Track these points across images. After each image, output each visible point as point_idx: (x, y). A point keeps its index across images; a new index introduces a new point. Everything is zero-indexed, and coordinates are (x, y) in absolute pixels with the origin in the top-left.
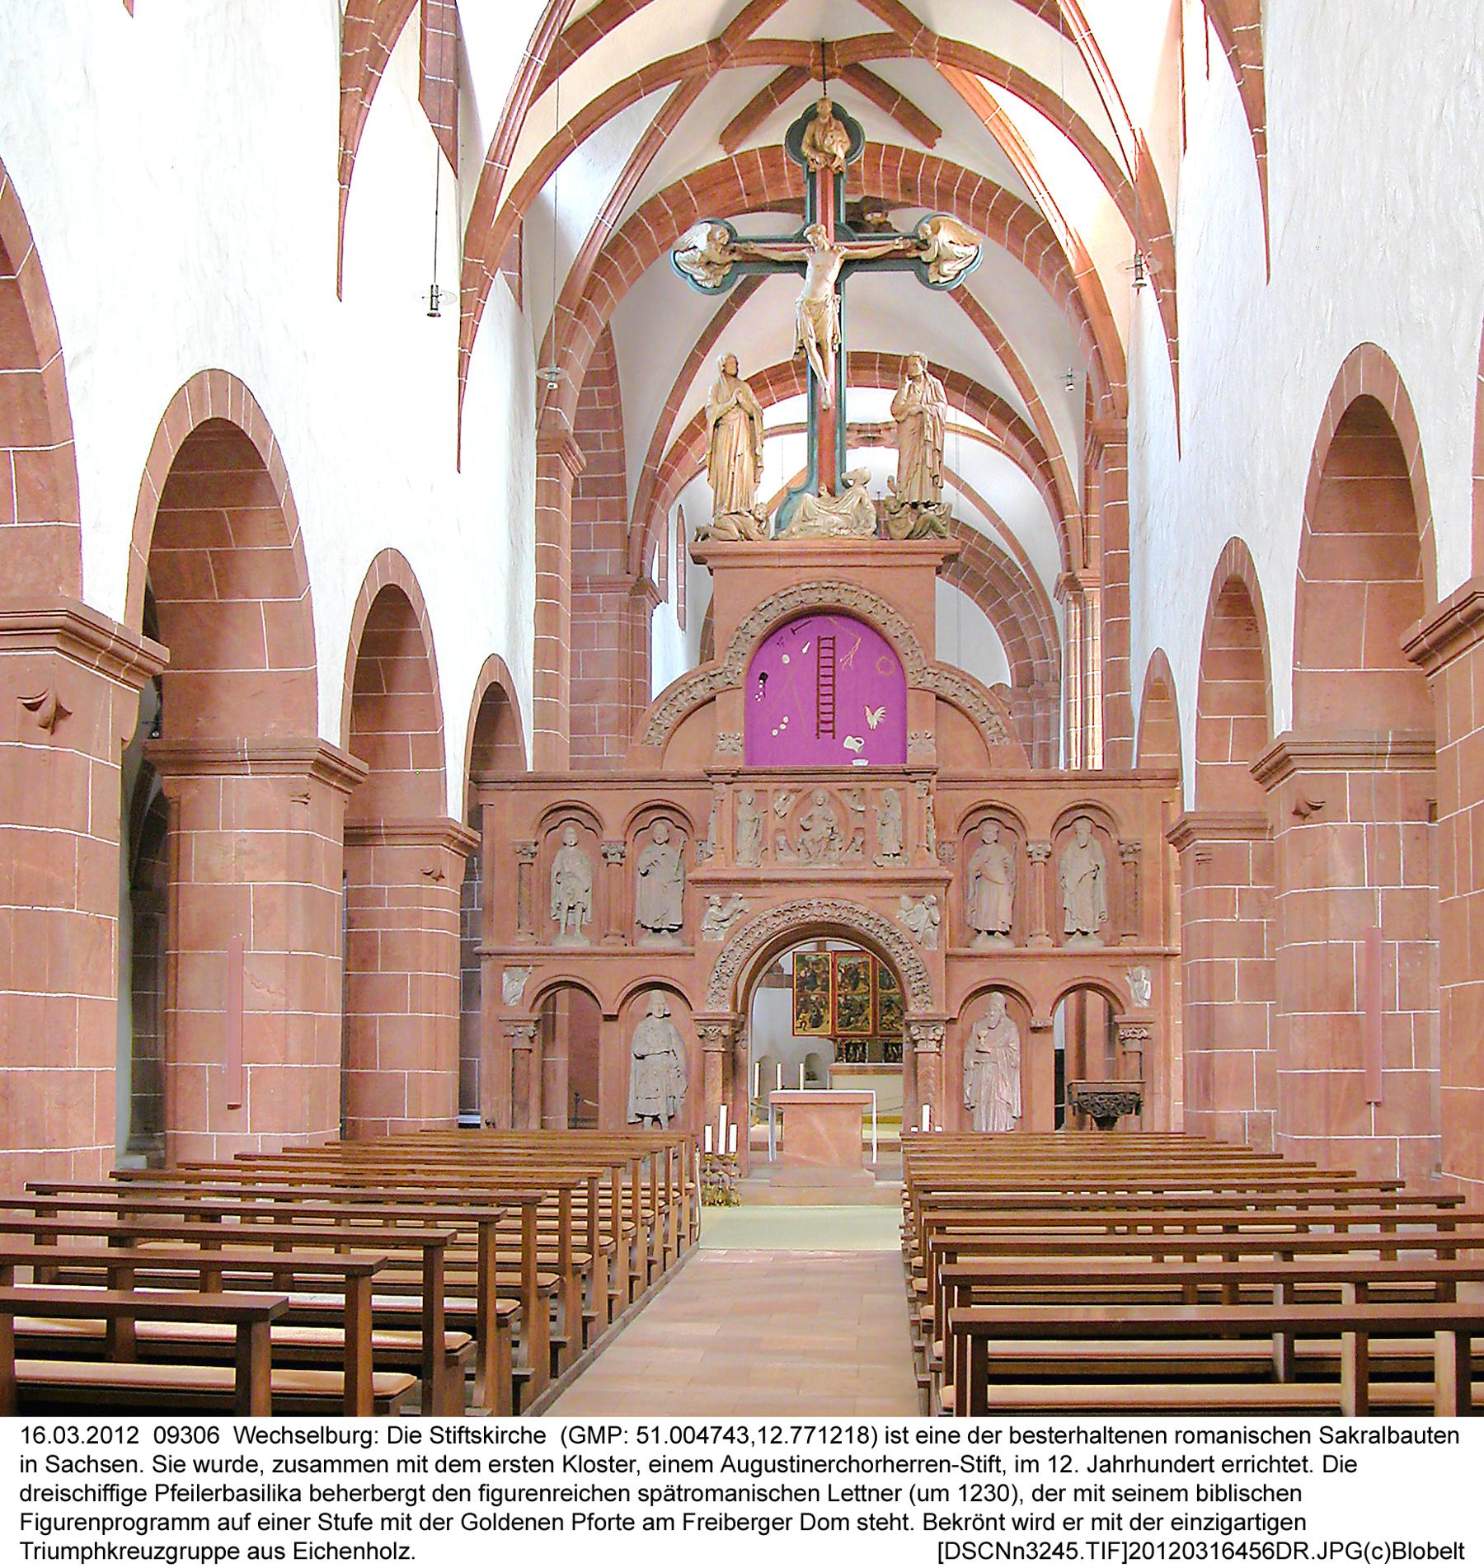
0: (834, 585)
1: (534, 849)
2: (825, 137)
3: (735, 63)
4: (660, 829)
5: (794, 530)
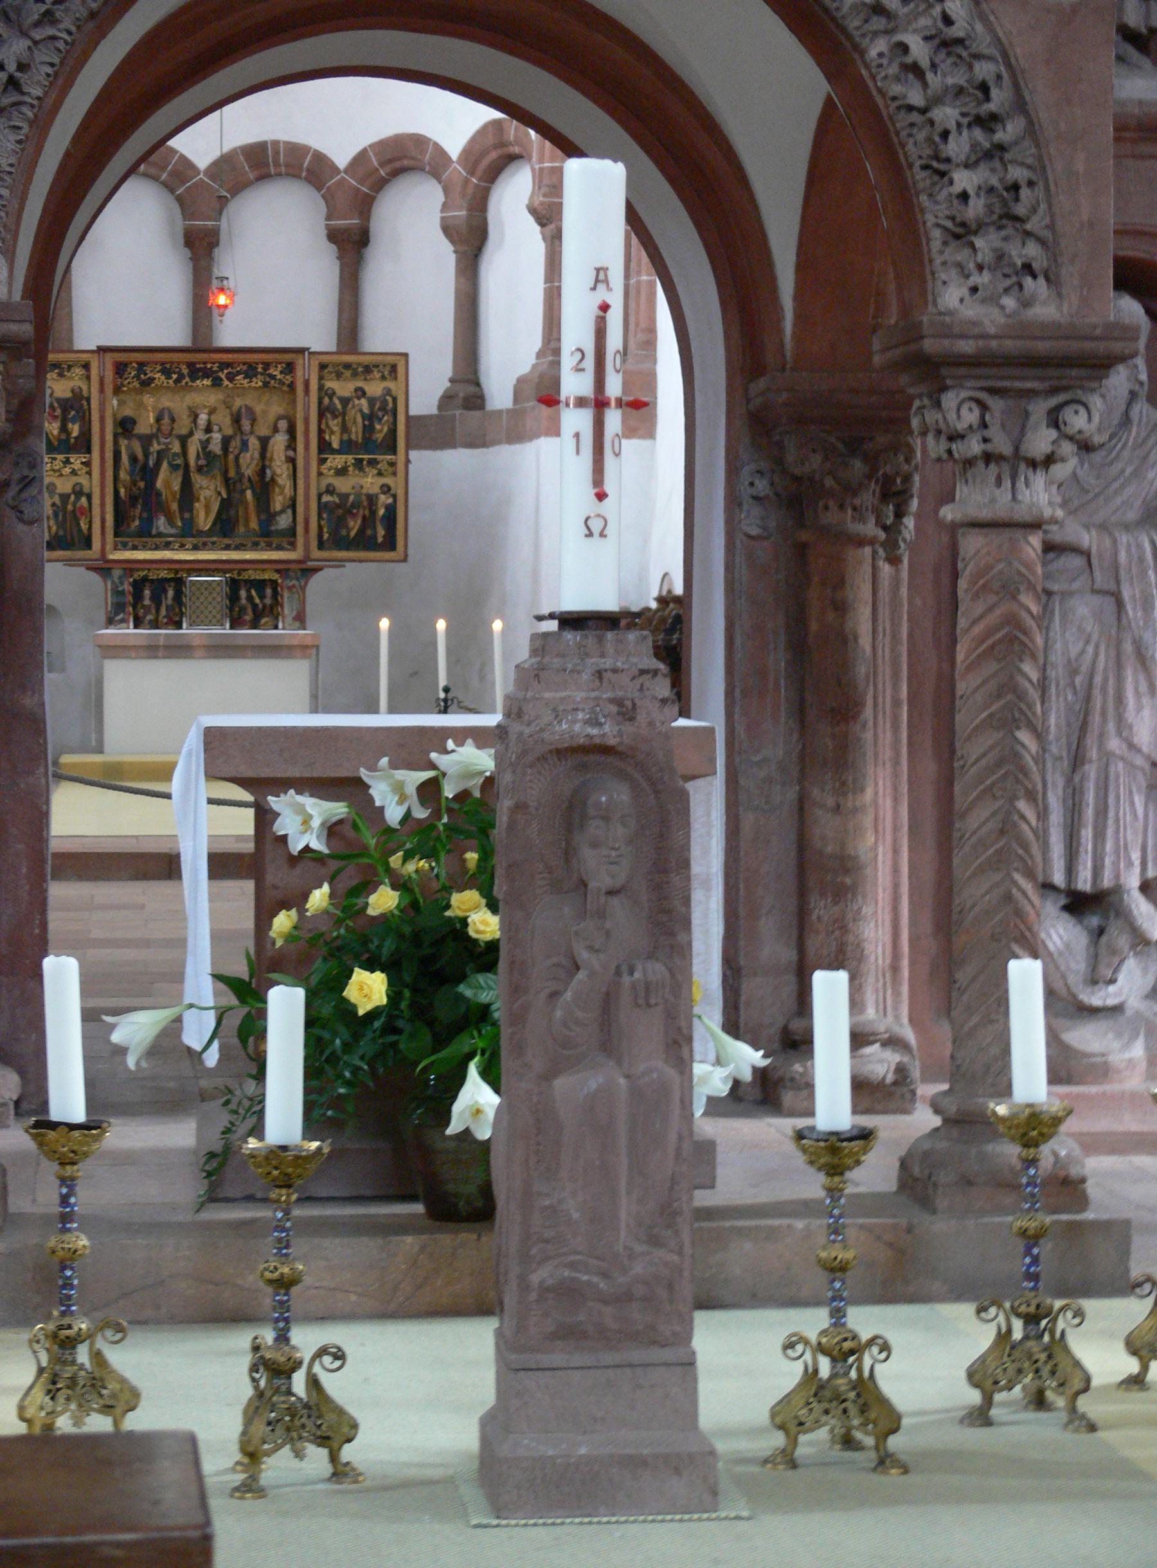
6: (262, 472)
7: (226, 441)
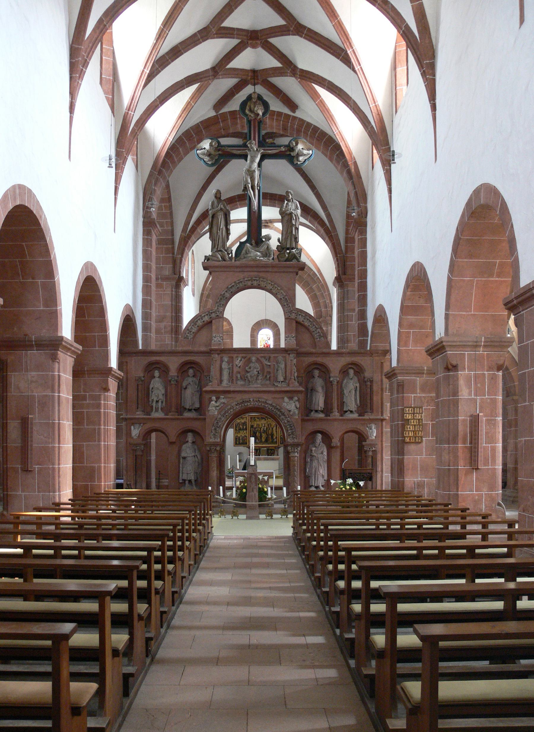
0: (257, 279)
1: (143, 379)
2: (255, 107)
3: (221, 77)
4: (191, 371)
6: (272, 433)
7: (267, 429)
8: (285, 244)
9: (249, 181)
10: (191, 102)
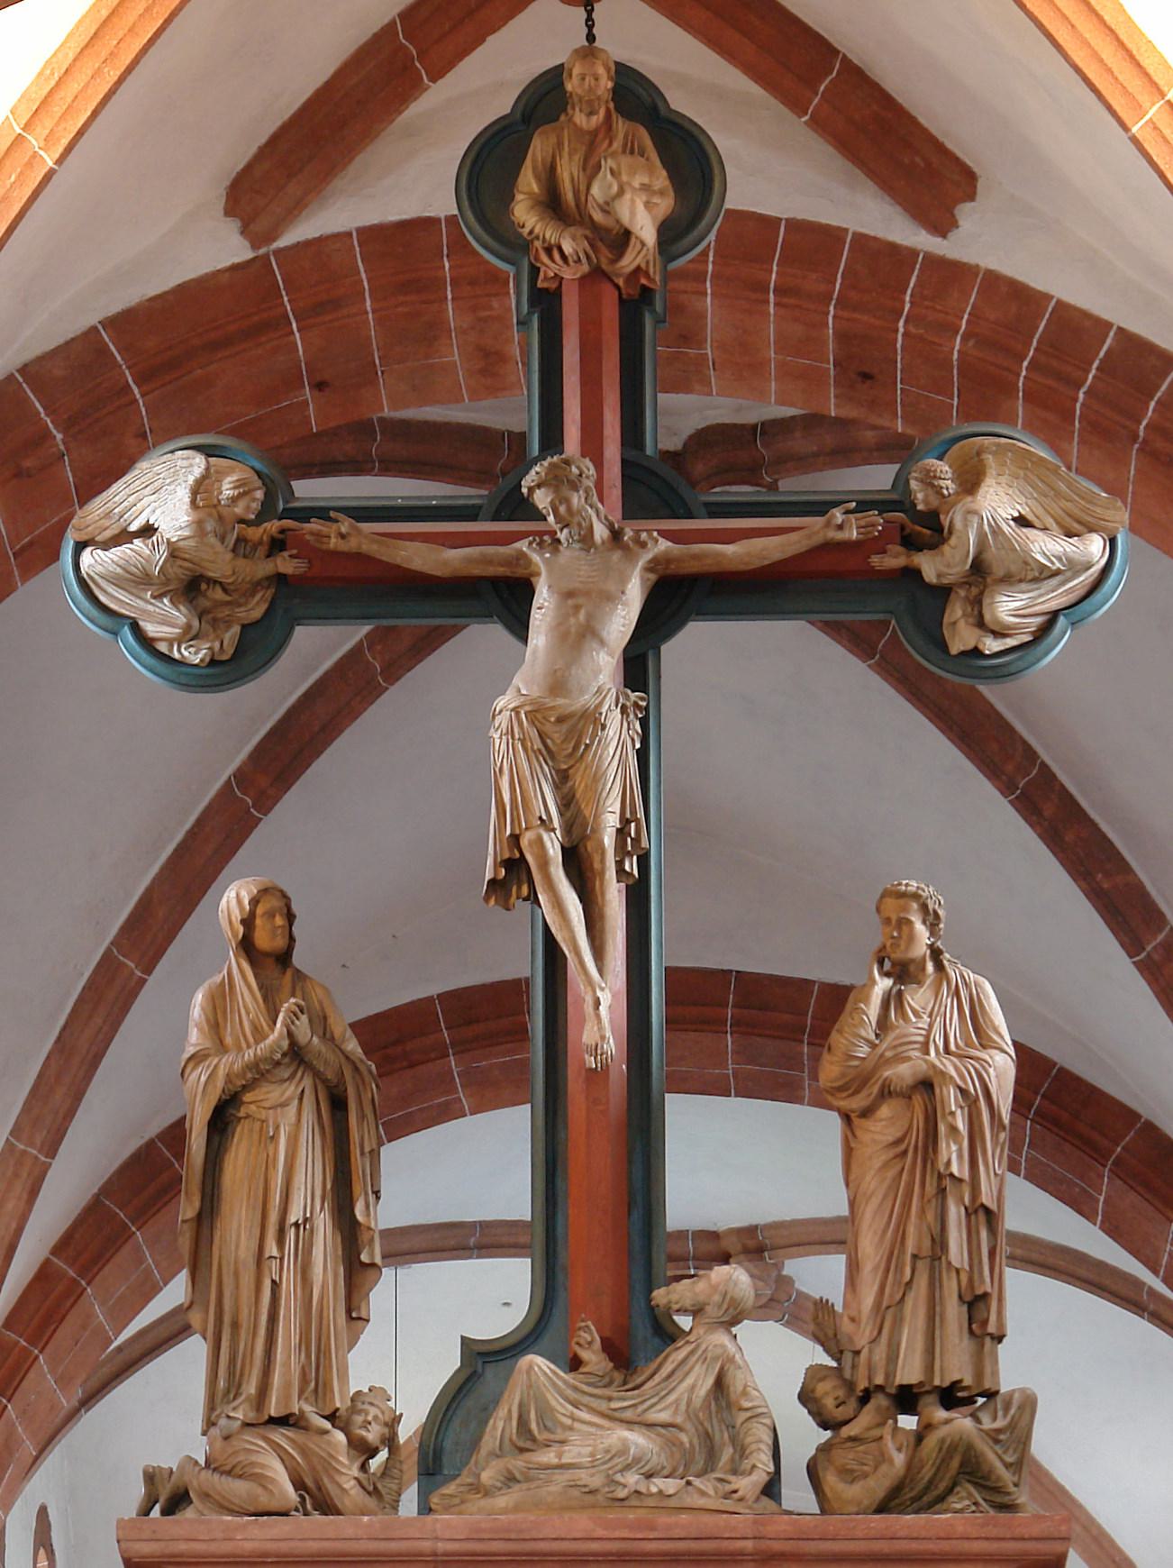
2: (591, 170)
5: (487, 1476)
8: (880, 1353)
9: (547, 801)
10: (33, 141)
